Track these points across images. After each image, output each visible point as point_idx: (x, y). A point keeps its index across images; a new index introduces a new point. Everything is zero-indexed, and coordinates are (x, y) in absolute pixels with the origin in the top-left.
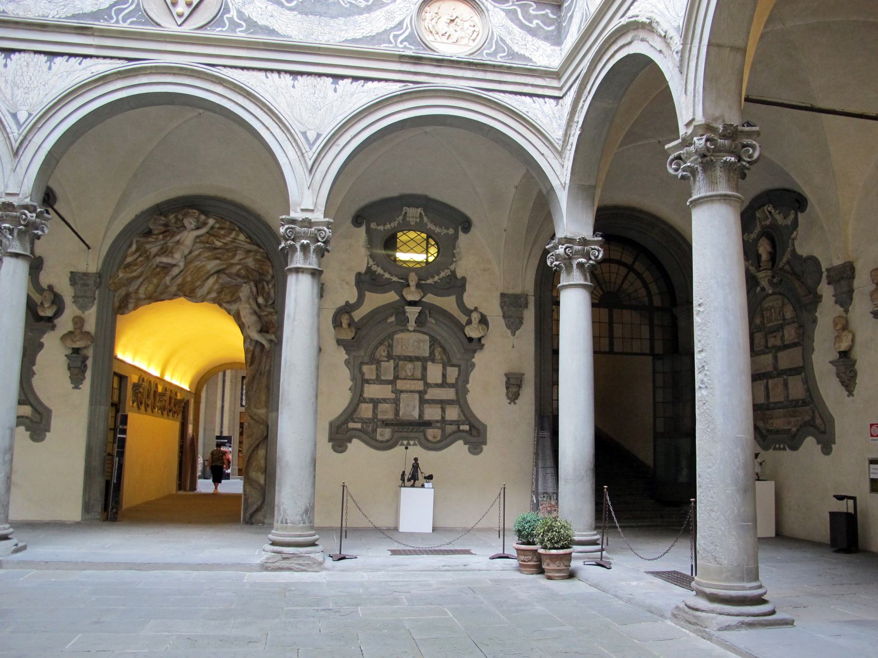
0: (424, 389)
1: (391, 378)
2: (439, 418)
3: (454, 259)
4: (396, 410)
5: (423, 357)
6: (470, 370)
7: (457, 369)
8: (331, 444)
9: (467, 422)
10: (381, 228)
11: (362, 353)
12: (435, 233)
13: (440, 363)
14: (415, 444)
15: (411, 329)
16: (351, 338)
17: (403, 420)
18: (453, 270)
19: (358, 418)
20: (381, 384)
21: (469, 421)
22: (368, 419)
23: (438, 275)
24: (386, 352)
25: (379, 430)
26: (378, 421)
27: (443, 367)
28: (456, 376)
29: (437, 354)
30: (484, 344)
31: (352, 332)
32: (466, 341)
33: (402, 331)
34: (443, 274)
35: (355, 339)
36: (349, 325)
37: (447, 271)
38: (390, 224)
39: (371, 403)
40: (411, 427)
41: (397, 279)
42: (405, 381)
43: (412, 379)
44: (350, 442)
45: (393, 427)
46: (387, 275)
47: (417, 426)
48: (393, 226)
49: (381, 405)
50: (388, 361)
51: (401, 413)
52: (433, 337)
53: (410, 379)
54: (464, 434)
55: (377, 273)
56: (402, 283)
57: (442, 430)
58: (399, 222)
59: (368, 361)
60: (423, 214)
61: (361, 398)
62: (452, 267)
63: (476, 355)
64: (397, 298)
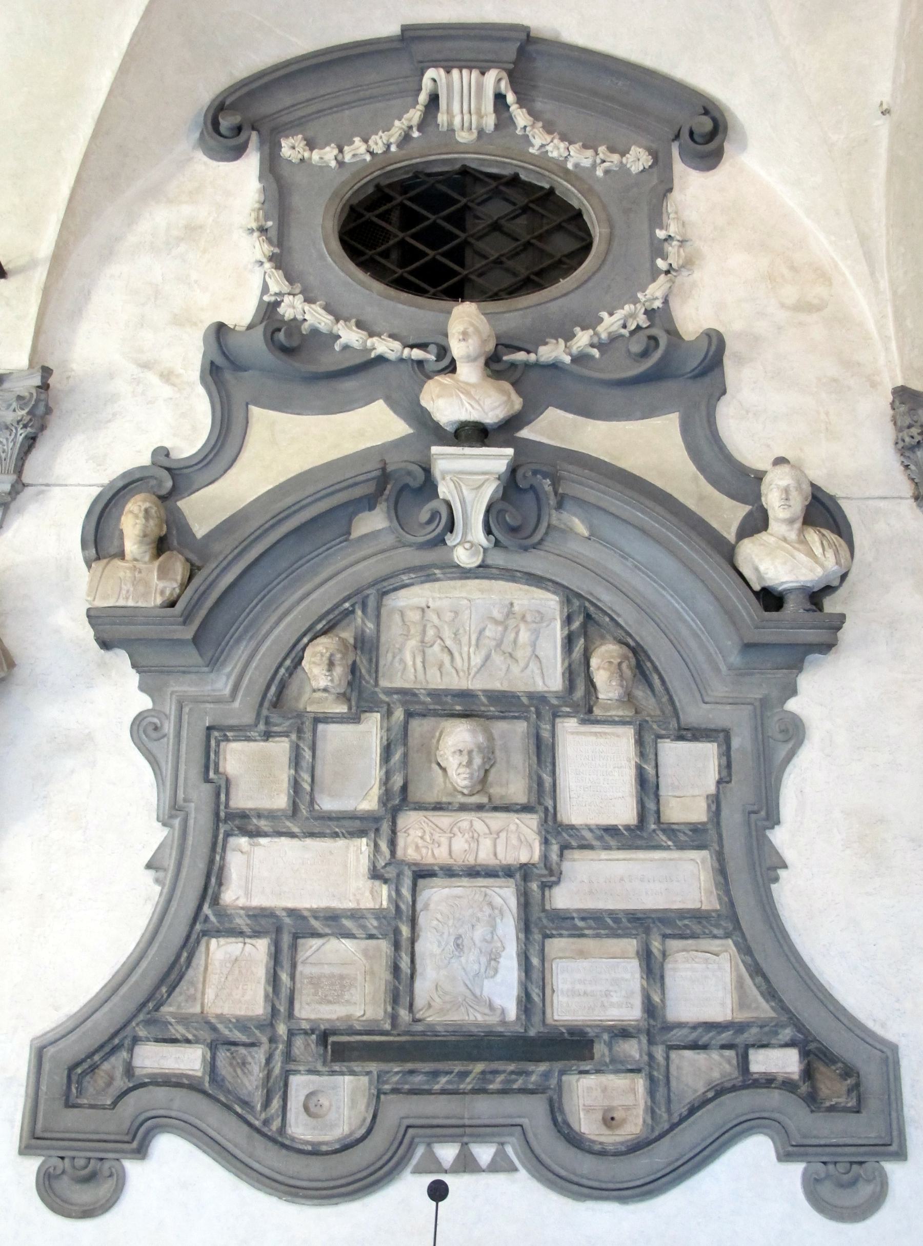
0: (545, 857)
1: (369, 803)
2: (632, 1013)
3: (661, 264)
4: (396, 969)
5: (531, 696)
6: (782, 751)
7: (709, 751)
8: (33, 1164)
9: (787, 1033)
10: (328, 154)
11: (222, 684)
12: (567, 171)
13: (623, 723)
14: (500, 1165)
15: (464, 557)
16: (159, 601)
17: (432, 1030)
18: (657, 304)
19: (184, 1020)
20: (312, 835)
21: (799, 1026)
22: (242, 1024)
23: (590, 323)
24: (338, 671)
25: (300, 1085)
26: (291, 1033)
27: (640, 742)
28: (712, 789)
29: (601, 677)
30: (842, 618)
31: (163, 573)
32: (750, 609)
33: (425, 574)
34: (610, 323)
35: (180, 606)
36: (161, 546)
37: (629, 308)
38: (366, 141)
39: (257, 934)
40: (479, 1067)
41: (397, 345)
42: (444, 820)
43: (480, 808)
44: (141, 1152)
45: (373, 1067)
46: (350, 336)
47: (510, 1059)
48: (379, 149)
49: (315, 943)
50: (354, 718)
51: (423, 988)
52: (579, 596)
53: (463, 808)
54: (775, 1098)
55: (305, 328)
56: (420, 363)
57: (652, 1079)
58: (406, 138)
59: (248, 718)
60: (511, 98)
61: (206, 909)
62: (655, 291)
63: (805, 681)
64: (399, 428)
